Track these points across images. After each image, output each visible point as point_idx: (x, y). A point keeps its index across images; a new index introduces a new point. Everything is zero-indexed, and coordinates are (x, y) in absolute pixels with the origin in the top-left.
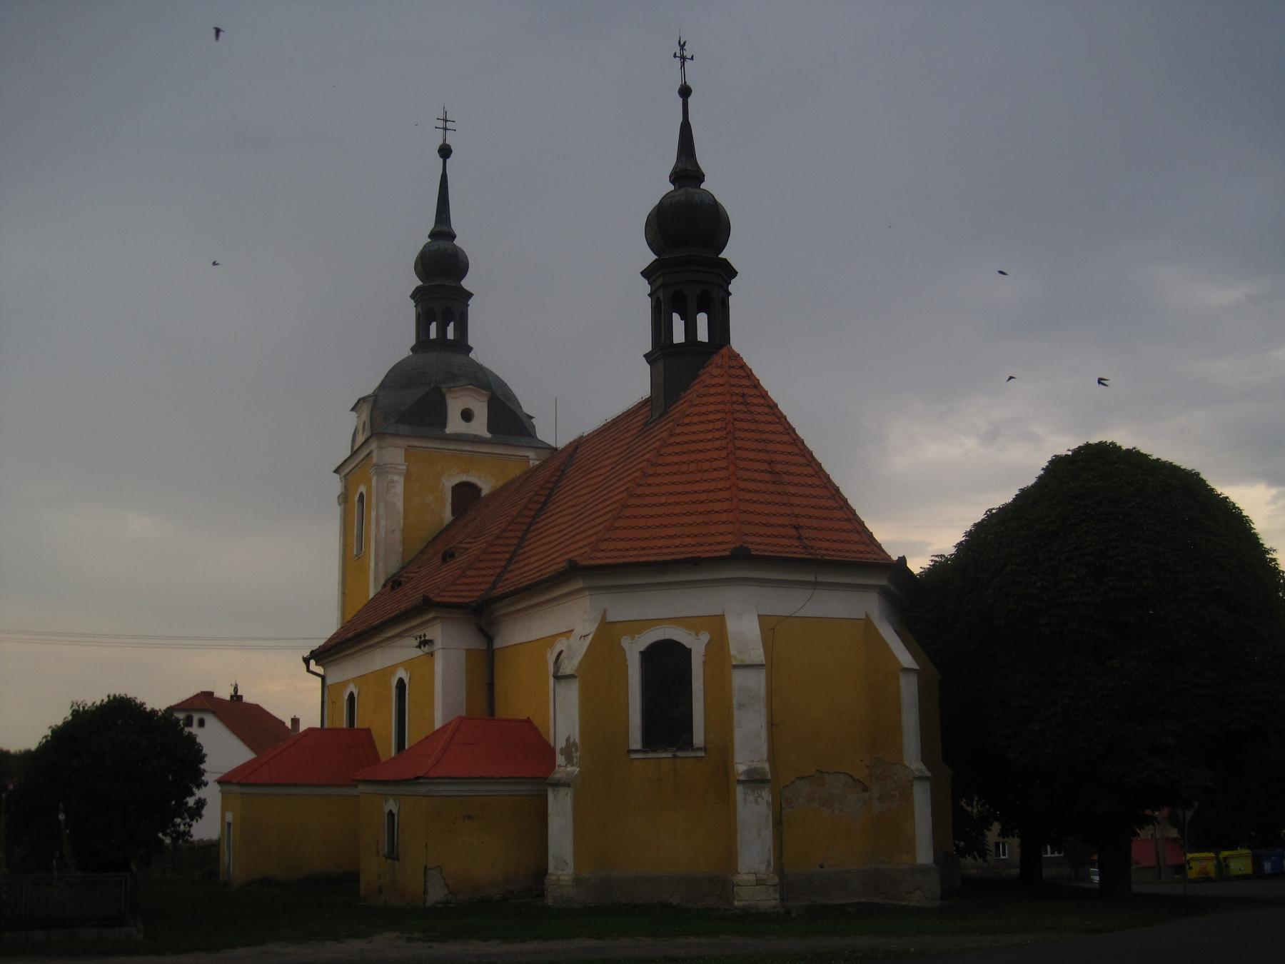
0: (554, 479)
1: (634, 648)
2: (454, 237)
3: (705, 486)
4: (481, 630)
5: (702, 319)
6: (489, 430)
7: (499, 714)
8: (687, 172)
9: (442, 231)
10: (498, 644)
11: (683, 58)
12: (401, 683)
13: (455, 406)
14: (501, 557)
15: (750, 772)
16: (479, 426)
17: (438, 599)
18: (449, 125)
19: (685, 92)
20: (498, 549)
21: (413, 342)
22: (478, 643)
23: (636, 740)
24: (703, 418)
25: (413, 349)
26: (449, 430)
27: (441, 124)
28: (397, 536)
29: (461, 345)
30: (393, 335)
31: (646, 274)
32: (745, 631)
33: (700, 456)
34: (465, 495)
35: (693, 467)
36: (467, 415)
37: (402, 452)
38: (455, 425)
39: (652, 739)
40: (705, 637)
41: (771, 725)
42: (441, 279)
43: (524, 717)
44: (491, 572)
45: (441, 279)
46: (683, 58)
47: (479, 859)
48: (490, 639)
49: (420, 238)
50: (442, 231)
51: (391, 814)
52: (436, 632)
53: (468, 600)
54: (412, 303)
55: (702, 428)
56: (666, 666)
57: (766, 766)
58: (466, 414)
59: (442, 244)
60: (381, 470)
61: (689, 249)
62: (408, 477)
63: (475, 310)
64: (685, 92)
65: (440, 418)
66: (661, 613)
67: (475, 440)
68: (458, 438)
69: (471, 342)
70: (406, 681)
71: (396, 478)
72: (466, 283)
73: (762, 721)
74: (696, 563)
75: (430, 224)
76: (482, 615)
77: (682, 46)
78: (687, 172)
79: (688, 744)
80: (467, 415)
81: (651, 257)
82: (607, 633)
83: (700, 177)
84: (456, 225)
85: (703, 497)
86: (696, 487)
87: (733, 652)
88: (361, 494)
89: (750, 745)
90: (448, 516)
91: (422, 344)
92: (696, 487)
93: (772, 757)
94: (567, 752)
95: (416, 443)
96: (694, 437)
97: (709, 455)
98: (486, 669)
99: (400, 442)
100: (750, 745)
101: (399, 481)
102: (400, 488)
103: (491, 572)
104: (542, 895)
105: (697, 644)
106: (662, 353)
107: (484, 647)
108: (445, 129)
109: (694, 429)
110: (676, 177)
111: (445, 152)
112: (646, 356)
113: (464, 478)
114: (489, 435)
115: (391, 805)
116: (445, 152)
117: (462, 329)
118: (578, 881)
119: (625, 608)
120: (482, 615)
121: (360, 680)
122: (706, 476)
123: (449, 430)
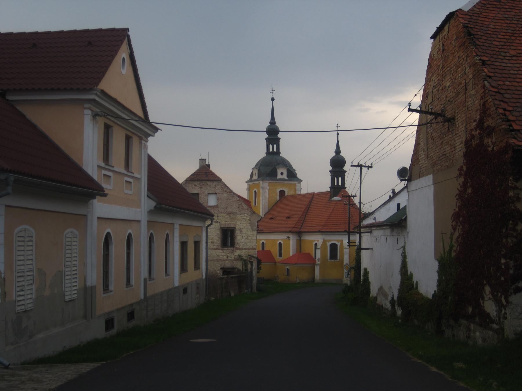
1: (329, 244)
5: (340, 178)
8: (338, 151)
9: (273, 122)
10: (302, 238)
12: (280, 244)
13: (279, 171)
16: (285, 176)
22: (299, 238)
23: (329, 258)
26: (278, 178)
27: (271, 91)
28: (267, 204)
29: (278, 153)
31: (330, 171)
32: (346, 242)
34: (282, 193)
36: (282, 174)
38: (279, 176)
39: (331, 258)
41: (350, 257)
42: (273, 134)
45: (273, 134)
47: (304, 276)
48: (300, 238)
50: (273, 122)
51: (288, 269)
52: (291, 236)
56: (334, 247)
60: (263, 188)
61: (338, 165)
62: (269, 189)
65: (276, 175)
66: (333, 239)
67: (284, 180)
68: (280, 180)
70: (282, 243)
74: (339, 232)
78: (338, 151)
80: (282, 174)
81: (331, 168)
82: (325, 242)
83: (340, 152)
84: (276, 119)
88: (255, 192)
89: (346, 260)
90: (278, 198)
91: (268, 153)
93: (349, 261)
94: (318, 260)
98: (300, 243)
99: (267, 182)
100: (346, 260)
101: (267, 191)
102: (267, 193)
104: (314, 281)
105: (339, 244)
106: (332, 186)
110: (336, 152)
111: (273, 99)
115: (288, 267)
116: (273, 99)
117: (278, 148)
118: (320, 279)
119: (327, 237)
121: (266, 240)
123: (278, 178)
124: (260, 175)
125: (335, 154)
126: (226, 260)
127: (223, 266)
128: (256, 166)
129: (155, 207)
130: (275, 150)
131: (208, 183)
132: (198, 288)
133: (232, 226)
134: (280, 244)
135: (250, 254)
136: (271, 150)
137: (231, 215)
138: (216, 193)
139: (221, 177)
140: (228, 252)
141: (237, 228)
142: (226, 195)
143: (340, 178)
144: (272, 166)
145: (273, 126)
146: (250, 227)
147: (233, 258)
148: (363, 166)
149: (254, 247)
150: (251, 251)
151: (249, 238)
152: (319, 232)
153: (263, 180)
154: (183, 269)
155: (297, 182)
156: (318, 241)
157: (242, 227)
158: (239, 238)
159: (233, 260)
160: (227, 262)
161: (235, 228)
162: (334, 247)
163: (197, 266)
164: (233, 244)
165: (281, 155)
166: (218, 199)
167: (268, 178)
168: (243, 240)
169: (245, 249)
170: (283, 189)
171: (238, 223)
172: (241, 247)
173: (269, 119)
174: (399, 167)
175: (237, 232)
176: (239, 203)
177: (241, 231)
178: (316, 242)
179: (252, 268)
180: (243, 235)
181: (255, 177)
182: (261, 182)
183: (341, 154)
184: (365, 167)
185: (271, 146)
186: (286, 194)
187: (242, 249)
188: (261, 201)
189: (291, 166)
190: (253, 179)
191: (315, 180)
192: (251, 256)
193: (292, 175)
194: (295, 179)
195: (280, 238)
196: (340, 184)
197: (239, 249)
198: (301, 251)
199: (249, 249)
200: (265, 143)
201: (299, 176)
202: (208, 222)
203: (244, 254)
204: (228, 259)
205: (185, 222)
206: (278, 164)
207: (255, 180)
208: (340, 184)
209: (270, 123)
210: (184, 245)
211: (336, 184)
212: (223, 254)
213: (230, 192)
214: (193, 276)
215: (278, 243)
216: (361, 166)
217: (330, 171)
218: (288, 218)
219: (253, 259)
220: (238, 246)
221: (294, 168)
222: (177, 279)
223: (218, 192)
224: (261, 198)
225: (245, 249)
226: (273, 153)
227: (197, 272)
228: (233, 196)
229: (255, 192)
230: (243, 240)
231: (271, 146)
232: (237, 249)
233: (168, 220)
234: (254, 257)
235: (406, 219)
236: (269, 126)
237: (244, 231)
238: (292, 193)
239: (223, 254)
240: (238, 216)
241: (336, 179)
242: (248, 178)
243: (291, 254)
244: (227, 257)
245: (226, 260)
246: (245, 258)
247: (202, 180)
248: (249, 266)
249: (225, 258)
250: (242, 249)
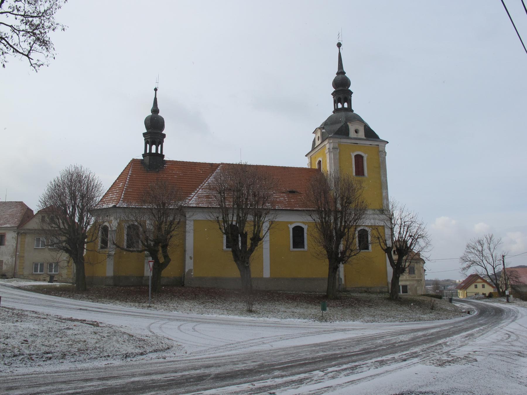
2: (345, 73)
6: (365, 136)
9: (341, 72)
21: (333, 110)
25: (334, 112)
29: (350, 109)
30: (326, 108)
38: (352, 134)
42: (342, 89)
45: (342, 89)
49: (333, 75)
50: (341, 72)
59: (340, 76)
63: (354, 98)
69: (353, 108)
75: (336, 70)
80: (356, 131)
84: (345, 70)
88: (320, 162)
91: (336, 110)
116: (339, 45)
167: (337, 136)
173: (335, 69)
194: (377, 140)
200: (331, 99)
201: (381, 137)
226: (343, 108)
229: (320, 162)
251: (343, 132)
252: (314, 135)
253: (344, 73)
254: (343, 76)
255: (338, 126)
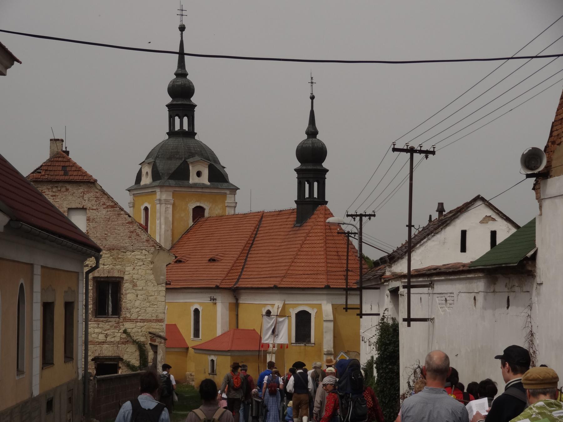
0: (255, 232)
3: (316, 261)
4: (235, 296)
5: (316, 184)
6: (209, 181)
7: (241, 326)
8: (312, 132)
10: (241, 301)
11: (312, 83)
12: (197, 312)
13: (193, 171)
14: (239, 268)
15: (328, 351)
16: (205, 179)
17: (221, 286)
18: (184, 13)
19: (312, 98)
20: (238, 264)
22: (233, 301)
24: (316, 234)
27: (179, 12)
29: (191, 134)
31: (296, 170)
33: (315, 249)
34: (198, 212)
35: (313, 253)
36: (199, 174)
37: (171, 193)
38: (193, 179)
40: (315, 310)
42: (181, 98)
43: (252, 329)
44: (236, 274)
45: (181, 98)
46: (312, 83)
51: (213, 361)
53: (230, 286)
54: (167, 109)
55: (316, 238)
56: (303, 319)
57: (332, 350)
58: (199, 175)
61: (312, 160)
62: (174, 205)
64: (312, 98)
65: (186, 177)
66: (302, 303)
67: (203, 186)
68: (195, 186)
70: (200, 310)
71: (169, 206)
72: (194, 100)
73: (332, 337)
76: (235, 292)
77: (312, 78)
78: (312, 132)
79: (309, 341)
80: (199, 174)
81: (298, 164)
85: (316, 265)
86: (314, 261)
87: (324, 316)
88: (146, 209)
90: (191, 223)
92: (314, 261)
95: (177, 189)
96: (313, 242)
97: (317, 249)
103: (236, 274)
106: (301, 201)
107: (235, 302)
108: (182, 15)
109: (313, 238)
111: (182, 28)
112: (295, 201)
113: (198, 204)
114: (209, 184)
116: (182, 28)
120: (235, 292)
122: (317, 257)
123: (191, 181)
124: (156, 175)
125: (305, 137)
126: (103, 343)
127: (97, 355)
128: (148, 157)
129: (7, 226)
130: (186, 127)
131: (68, 186)
132: (70, 400)
133: (116, 274)
134: (197, 312)
135: (151, 330)
136: (177, 127)
137: (115, 252)
138: (84, 209)
139: (95, 177)
140: (107, 326)
141: (126, 277)
142: (104, 212)
143: (316, 184)
144: (181, 161)
145: (180, 81)
146: (152, 277)
147: (117, 339)
148: (416, 151)
149: (161, 316)
150: (154, 325)
151: (151, 298)
152: (275, 288)
153: (161, 186)
154: (47, 360)
155: (228, 192)
156: (273, 305)
157: (135, 276)
158: (130, 299)
159: (118, 343)
160: (105, 346)
161: (123, 278)
162: (303, 319)
163: (69, 356)
164: (117, 311)
165: (196, 137)
166: (88, 220)
167: (172, 182)
168: (137, 303)
169: (143, 321)
170: (202, 205)
171: (128, 269)
172: (134, 316)
174: (525, 148)
175: (126, 286)
176: (132, 229)
177: (135, 285)
178: (269, 308)
179: (155, 359)
180: (138, 292)
181: (146, 180)
182: (158, 190)
183: (318, 137)
184: (421, 152)
185: (177, 120)
186: (207, 214)
187: (136, 321)
188: (158, 228)
189: (216, 160)
190: (142, 183)
191: (264, 185)
192: (154, 336)
193: (218, 176)
194: (225, 185)
195: (197, 301)
196: (316, 195)
197: (131, 320)
198: (238, 328)
199: (150, 321)
200: (165, 112)
202: (91, 262)
203: (139, 332)
204: (109, 339)
205: (51, 263)
206: (192, 155)
207: (146, 187)
208: (316, 195)
209: (176, 74)
210: (48, 307)
211: (307, 195)
212: (97, 330)
213: (112, 207)
214: (62, 374)
215: (192, 309)
216: (411, 151)
217: (296, 170)
218: (212, 260)
219: (158, 340)
220: (128, 315)
221: (223, 163)
222: (37, 382)
223: (88, 205)
224: (158, 222)
225: (143, 321)
226: (182, 134)
227: (69, 365)
228: (119, 215)
229: (146, 209)
230: (137, 303)
231: (177, 120)
232: (126, 320)
233: (22, 256)
234: (160, 337)
235: (534, 256)
236: (174, 81)
237: (140, 284)
238: (217, 211)
239: (97, 330)
240: (128, 253)
241: (307, 186)
242: (132, 182)
243: (219, 332)
244: (107, 335)
245: (103, 343)
246: (142, 339)
247: (58, 182)
248: (151, 355)
249: (101, 338)
250: (136, 321)
251: (181, 175)
252: (140, 166)
253: (185, 75)
254: (184, 79)
255: (175, 165)
